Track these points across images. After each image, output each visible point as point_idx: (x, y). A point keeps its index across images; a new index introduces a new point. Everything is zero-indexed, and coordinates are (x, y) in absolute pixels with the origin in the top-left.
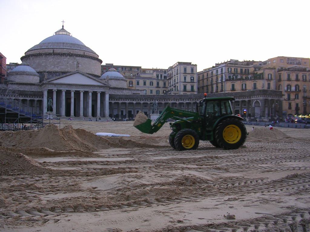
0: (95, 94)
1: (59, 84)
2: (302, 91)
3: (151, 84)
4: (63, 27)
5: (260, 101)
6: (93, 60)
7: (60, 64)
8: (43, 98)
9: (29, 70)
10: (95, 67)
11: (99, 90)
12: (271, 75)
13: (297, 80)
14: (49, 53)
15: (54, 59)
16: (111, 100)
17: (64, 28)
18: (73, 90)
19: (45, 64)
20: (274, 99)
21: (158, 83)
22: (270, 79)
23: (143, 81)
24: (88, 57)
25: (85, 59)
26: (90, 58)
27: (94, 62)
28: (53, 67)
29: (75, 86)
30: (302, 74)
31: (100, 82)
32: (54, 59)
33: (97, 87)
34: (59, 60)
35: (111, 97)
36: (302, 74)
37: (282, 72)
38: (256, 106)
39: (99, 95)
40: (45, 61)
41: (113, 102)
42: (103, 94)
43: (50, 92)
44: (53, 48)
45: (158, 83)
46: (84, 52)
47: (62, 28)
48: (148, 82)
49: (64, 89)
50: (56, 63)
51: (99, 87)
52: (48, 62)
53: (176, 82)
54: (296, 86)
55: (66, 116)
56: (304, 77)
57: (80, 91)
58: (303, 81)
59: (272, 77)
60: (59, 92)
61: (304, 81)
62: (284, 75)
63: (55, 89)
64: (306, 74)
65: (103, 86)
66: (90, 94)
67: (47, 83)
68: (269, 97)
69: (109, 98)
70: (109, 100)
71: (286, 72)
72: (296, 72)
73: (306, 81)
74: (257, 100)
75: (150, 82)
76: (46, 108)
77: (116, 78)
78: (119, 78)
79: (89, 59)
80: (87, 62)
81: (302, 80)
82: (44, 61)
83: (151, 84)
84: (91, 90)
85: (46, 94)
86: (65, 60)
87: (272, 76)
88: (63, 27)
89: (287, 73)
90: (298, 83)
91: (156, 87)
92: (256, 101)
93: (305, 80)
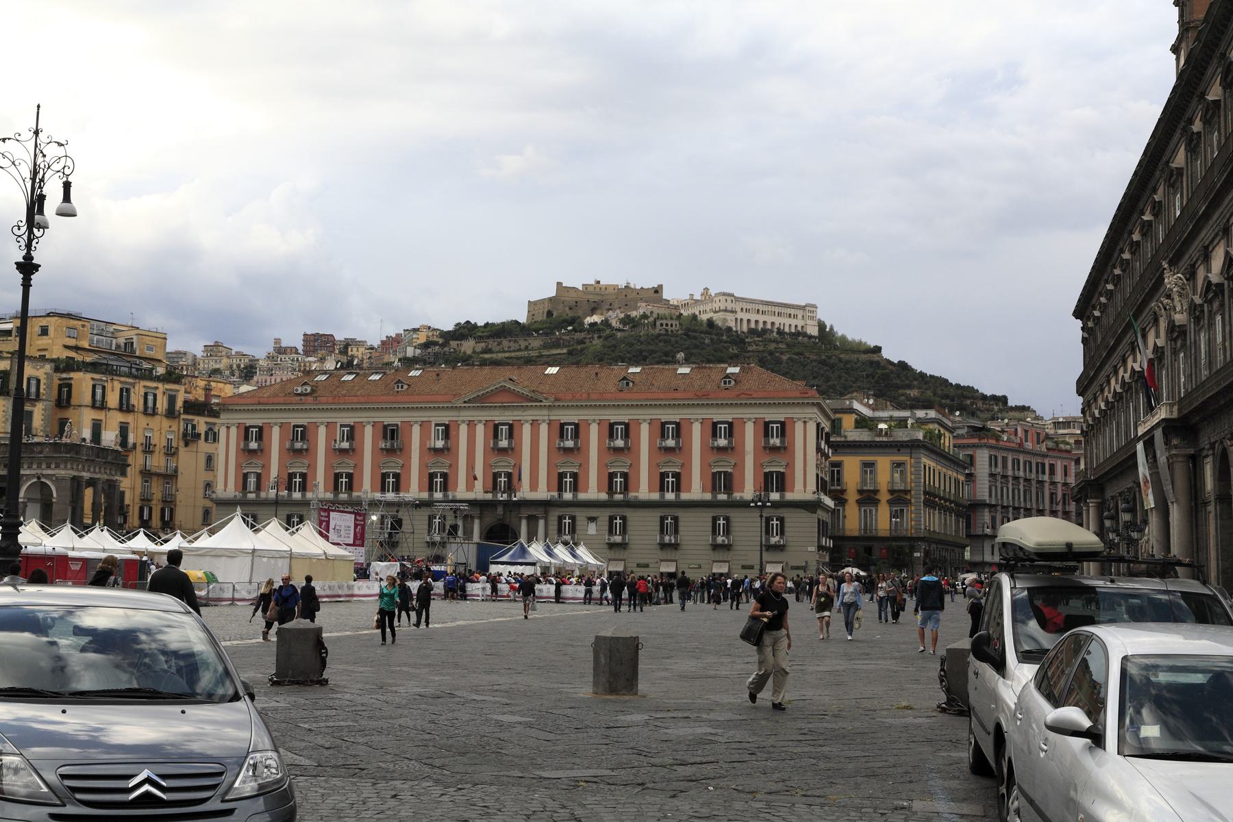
2: (139, 449)
5: (52, 481)
12: (38, 381)
13: (125, 407)
20: (98, 476)
22: (33, 397)
30: (144, 387)
36: (121, 382)
37: (75, 376)
38: (30, 500)
54: (124, 430)
56: (150, 398)
58: (145, 413)
59: (42, 390)
61: (150, 414)
62: (83, 382)
64: (157, 388)
68: (83, 470)
71: (89, 376)
72: (122, 379)
73: (154, 413)
74: (39, 478)
81: (141, 408)
87: (42, 387)
89: (93, 379)
90: (129, 418)
92: (35, 480)
93: (98, 404)
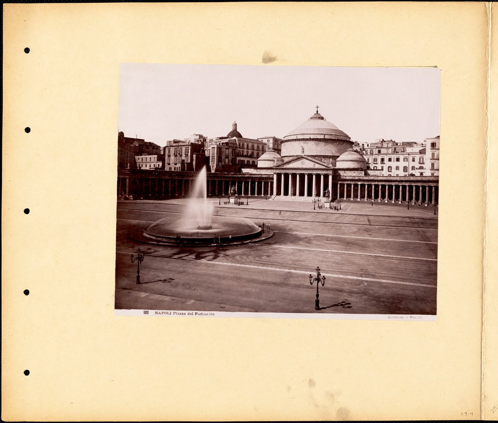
0: (318, 176)
4: (317, 112)
8: (273, 180)
17: (318, 113)
39: (322, 177)
42: (326, 177)
43: (279, 175)
46: (324, 136)
47: (316, 113)
57: (296, 173)
60: (286, 176)
85: (275, 177)
88: (317, 112)
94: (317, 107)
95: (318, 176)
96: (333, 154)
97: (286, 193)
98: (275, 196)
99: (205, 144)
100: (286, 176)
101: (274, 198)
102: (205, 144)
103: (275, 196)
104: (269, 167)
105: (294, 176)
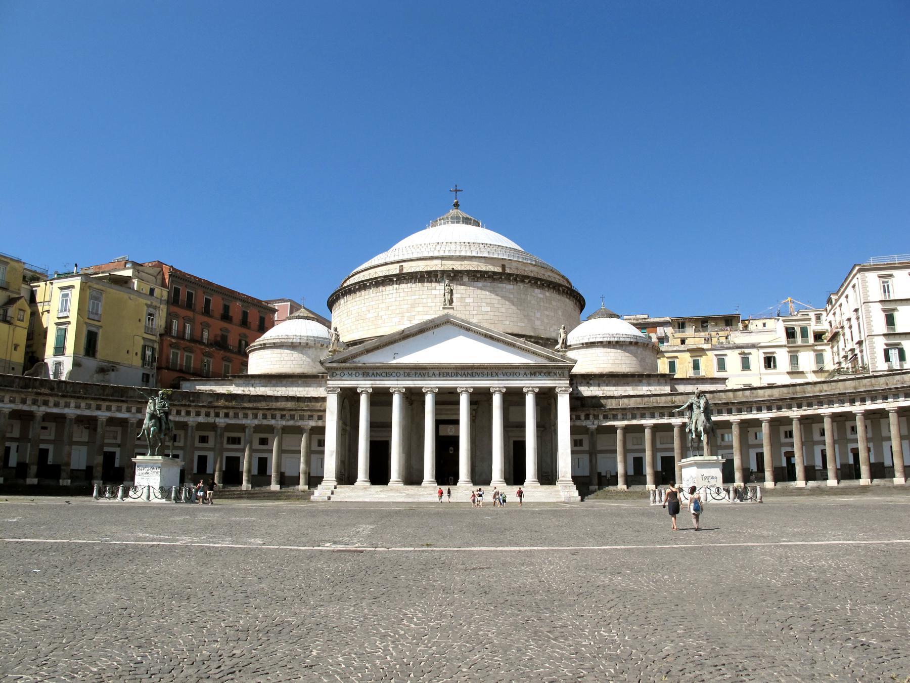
0: (513, 399)
1: (378, 368)
3: (769, 361)
6: (537, 291)
7: (417, 309)
8: (321, 418)
9: (304, 333)
10: (547, 313)
11: (530, 385)
14: (384, 277)
15: (402, 294)
16: (574, 417)
18: (430, 385)
19: (376, 314)
21: (794, 360)
23: (740, 354)
24: (515, 280)
25: (504, 285)
26: (523, 281)
27: (541, 296)
28: (397, 319)
29: (437, 372)
31: (534, 353)
32: (402, 294)
33: (522, 372)
34: (417, 297)
35: (579, 404)
40: (374, 303)
41: (592, 425)
42: (546, 399)
43: (349, 399)
44: (398, 262)
45: (794, 360)
48: (757, 358)
49: (396, 385)
50: (406, 306)
51: (528, 372)
52: (383, 305)
53: (856, 339)
55: (542, 484)
60: (381, 399)
63: (364, 385)
65: (546, 367)
66: (497, 400)
67: (334, 365)
69: (573, 409)
70: (571, 419)
75: (763, 356)
76: (332, 455)
77: (612, 339)
78: (622, 339)
79: (521, 285)
80: (512, 296)
82: (371, 303)
83: (769, 361)
84: (496, 384)
86: (434, 292)
91: (788, 373)
94: (456, 191)
95: (513, 399)
96: (535, 329)
97: (379, 475)
98: (335, 488)
99: (34, 289)
100: (381, 399)
101: (332, 493)
102: (34, 289)
103: (335, 488)
104: (298, 370)
105: (414, 398)
